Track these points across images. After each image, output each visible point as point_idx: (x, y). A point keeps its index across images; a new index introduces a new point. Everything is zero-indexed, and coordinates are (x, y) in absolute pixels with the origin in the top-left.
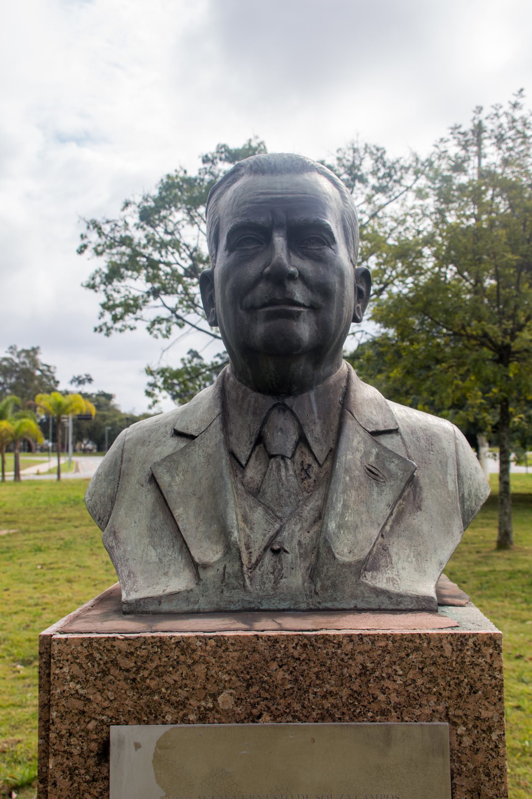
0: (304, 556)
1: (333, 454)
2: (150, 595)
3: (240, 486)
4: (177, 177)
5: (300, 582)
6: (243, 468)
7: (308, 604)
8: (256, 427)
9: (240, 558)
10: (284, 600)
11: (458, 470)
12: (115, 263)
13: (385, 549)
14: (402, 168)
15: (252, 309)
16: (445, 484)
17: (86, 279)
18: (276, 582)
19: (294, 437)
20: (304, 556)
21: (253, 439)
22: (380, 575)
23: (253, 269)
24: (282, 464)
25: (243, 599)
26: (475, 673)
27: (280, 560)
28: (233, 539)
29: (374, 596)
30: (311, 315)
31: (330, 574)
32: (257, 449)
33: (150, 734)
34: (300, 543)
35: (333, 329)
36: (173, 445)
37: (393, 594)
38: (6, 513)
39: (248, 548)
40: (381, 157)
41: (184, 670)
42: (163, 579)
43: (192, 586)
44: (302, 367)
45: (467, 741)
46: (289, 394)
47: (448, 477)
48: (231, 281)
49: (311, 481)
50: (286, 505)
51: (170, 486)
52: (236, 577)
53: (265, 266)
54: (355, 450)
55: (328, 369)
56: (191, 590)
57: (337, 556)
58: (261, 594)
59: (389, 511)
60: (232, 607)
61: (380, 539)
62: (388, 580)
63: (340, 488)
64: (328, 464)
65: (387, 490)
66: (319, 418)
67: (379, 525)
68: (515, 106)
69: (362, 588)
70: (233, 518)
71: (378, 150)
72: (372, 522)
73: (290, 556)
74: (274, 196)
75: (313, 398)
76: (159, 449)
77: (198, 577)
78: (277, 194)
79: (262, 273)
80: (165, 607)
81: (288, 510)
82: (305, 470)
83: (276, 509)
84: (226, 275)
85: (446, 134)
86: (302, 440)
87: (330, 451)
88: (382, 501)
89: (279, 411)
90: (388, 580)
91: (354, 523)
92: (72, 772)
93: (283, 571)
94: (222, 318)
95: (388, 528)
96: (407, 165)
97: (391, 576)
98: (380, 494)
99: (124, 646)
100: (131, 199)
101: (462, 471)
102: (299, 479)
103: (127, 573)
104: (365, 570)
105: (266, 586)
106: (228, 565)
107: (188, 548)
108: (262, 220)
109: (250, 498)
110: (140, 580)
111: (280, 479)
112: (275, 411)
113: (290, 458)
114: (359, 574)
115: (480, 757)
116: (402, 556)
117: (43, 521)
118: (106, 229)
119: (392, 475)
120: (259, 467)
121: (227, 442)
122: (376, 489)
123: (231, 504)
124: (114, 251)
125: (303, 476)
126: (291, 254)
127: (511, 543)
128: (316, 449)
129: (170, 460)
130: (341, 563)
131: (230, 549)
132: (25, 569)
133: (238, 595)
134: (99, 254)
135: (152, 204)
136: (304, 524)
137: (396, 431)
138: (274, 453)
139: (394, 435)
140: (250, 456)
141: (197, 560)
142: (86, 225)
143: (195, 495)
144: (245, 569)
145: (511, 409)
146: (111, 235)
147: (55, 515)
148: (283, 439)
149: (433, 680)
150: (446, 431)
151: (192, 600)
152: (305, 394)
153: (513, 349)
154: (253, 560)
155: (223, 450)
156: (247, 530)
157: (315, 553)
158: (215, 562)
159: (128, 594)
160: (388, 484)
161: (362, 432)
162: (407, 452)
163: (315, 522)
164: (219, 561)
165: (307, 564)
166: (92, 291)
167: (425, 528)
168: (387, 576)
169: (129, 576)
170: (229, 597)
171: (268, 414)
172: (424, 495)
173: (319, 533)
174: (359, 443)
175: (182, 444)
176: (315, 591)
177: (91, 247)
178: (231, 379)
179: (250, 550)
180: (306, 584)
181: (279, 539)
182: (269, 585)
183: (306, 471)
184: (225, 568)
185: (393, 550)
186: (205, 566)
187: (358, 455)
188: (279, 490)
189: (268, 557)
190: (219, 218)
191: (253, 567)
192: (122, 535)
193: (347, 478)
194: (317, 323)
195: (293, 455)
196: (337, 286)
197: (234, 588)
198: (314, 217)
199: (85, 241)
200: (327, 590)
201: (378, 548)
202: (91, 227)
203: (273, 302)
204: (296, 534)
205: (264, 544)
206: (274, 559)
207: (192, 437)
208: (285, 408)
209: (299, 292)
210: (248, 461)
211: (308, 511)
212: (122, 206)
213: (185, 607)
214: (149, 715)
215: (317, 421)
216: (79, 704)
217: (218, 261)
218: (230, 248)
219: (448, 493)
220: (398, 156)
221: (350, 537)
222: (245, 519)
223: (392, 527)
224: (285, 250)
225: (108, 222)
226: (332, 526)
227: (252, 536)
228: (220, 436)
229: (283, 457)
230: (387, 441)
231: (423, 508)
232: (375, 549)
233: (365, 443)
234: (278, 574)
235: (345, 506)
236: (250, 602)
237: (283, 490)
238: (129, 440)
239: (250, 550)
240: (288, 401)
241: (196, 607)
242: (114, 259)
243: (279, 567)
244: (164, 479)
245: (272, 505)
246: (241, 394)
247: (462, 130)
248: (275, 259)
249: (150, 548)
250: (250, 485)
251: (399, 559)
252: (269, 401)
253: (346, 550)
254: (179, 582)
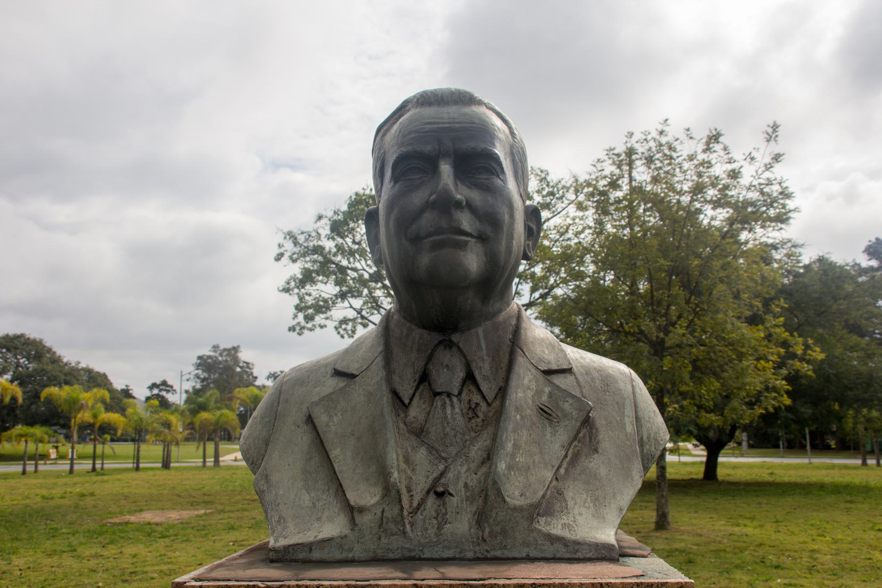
0: (470, 499)
1: (503, 392)
2: (300, 541)
3: (402, 425)
4: (364, 195)
5: (467, 528)
6: (406, 407)
7: (475, 552)
8: (421, 364)
9: (400, 501)
10: (449, 548)
11: (636, 412)
12: (309, 269)
13: (560, 493)
14: (563, 187)
15: (416, 240)
16: (623, 426)
17: (282, 283)
18: (440, 528)
19: (461, 374)
20: (470, 499)
21: (417, 377)
22: (554, 521)
23: (418, 198)
24: (448, 402)
25: (402, 547)
27: (444, 504)
28: (392, 479)
29: (548, 543)
30: (479, 245)
31: (499, 519)
32: (421, 387)
34: (466, 485)
35: (502, 263)
36: (332, 384)
37: (569, 541)
38: (205, 495)
39: (409, 490)
40: (545, 178)
42: (316, 525)
43: (346, 531)
44: (470, 300)
46: (456, 329)
47: (626, 418)
48: (396, 211)
49: (479, 420)
50: (452, 445)
51: (327, 425)
52: (396, 522)
53: (431, 195)
54: (525, 389)
55: (497, 305)
56: (346, 536)
57: (507, 499)
58: (422, 541)
59: (563, 453)
60: (391, 556)
61: (554, 482)
62: (564, 525)
63: (511, 427)
64: (497, 403)
65: (561, 431)
66: (488, 355)
67: (553, 467)
68: (661, 133)
69: (535, 534)
70: (393, 457)
71: (542, 171)
72: (546, 464)
73: (455, 500)
74: (441, 125)
75: (481, 334)
76: (318, 389)
77: (353, 522)
78: (443, 123)
79: (427, 202)
80: (316, 555)
81: (453, 450)
82: (473, 410)
83: (441, 449)
84: (390, 207)
85: (602, 155)
86: (470, 377)
87: (500, 389)
88: (556, 441)
89: (445, 348)
90: (564, 526)
91: (526, 462)
93: (448, 516)
94: (386, 252)
95: (562, 471)
96: (568, 185)
97: (567, 522)
98: (553, 434)
100: (324, 213)
101: (640, 414)
102: (466, 419)
103: (276, 518)
104: (538, 515)
105: (429, 532)
106: (386, 508)
107: (343, 491)
108: (428, 148)
109: (413, 438)
110: (291, 526)
111: (446, 417)
112: (441, 348)
113: (457, 396)
114: (531, 519)
116: (578, 501)
117: (237, 502)
118: (301, 239)
119: (566, 415)
120: (424, 406)
121: (389, 379)
122: (549, 429)
123: (392, 443)
124: (308, 259)
125: (471, 415)
126: (458, 183)
127: (668, 524)
128: (484, 387)
129: (329, 400)
130: (512, 507)
131: (389, 492)
132: (218, 545)
134: (294, 261)
135: (341, 217)
136: (471, 465)
137: (569, 371)
138: (439, 390)
139: (568, 375)
140: (414, 395)
141: (352, 503)
142: (283, 236)
143: (353, 435)
144: (405, 513)
145: (666, 400)
146: (306, 245)
147: (248, 497)
148: (448, 375)
150: (623, 374)
151: (346, 547)
152: (473, 331)
153: (667, 345)
154: (415, 504)
155: (384, 388)
156: (409, 472)
157: (483, 496)
158: (373, 505)
159: (276, 540)
160: (562, 424)
161: (533, 370)
162: (582, 392)
163: (483, 463)
164: (377, 504)
165: (474, 509)
166: (287, 294)
167: (603, 471)
168: (563, 521)
169: (279, 521)
170: (388, 544)
171: (434, 351)
172: (601, 437)
173: (487, 475)
174: (530, 381)
175: (341, 383)
176: (483, 538)
177: (287, 255)
178: (395, 316)
179: (412, 493)
180: (472, 530)
181: (443, 480)
182: (432, 531)
183: (473, 410)
184: (383, 512)
185: (569, 494)
186: (362, 510)
187: (530, 394)
188: (444, 428)
189: (431, 500)
190: (385, 152)
191: (415, 511)
192: (275, 478)
193: (518, 417)
194: (486, 254)
195: (460, 393)
196: (507, 217)
197: (393, 535)
198: (482, 146)
199: (282, 250)
200: (496, 537)
201: (552, 492)
202: (288, 237)
204: (462, 477)
205: (427, 487)
206: (438, 503)
207: (353, 376)
208: (450, 345)
209: (466, 221)
210: (411, 400)
211: (476, 451)
212: (314, 219)
213: (338, 556)
215: (486, 358)
217: (383, 194)
218: (395, 179)
219: (626, 435)
220: (560, 177)
221: (521, 479)
222: (407, 460)
223: (567, 470)
224: (452, 177)
225: (302, 233)
226: (502, 466)
227: (414, 478)
228: (382, 374)
229: (449, 395)
230: (559, 380)
231: (600, 451)
232: (549, 492)
233: (537, 381)
234: (442, 519)
235: (516, 446)
236: (410, 550)
237: (448, 429)
238: (287, 381)
239: (412, 493)
240: (455, 338)
241: (350, 555)
242: (307, 266)
243: (443, 511)
244: (322, 419)
245: (436, 445)
246: (405, 331)
247: (616, 152)
248: (441, 186)
249: (304, 491)
250: (414, 425)
251: (575, 504)
253: (517, 493)
254: (332, 527)
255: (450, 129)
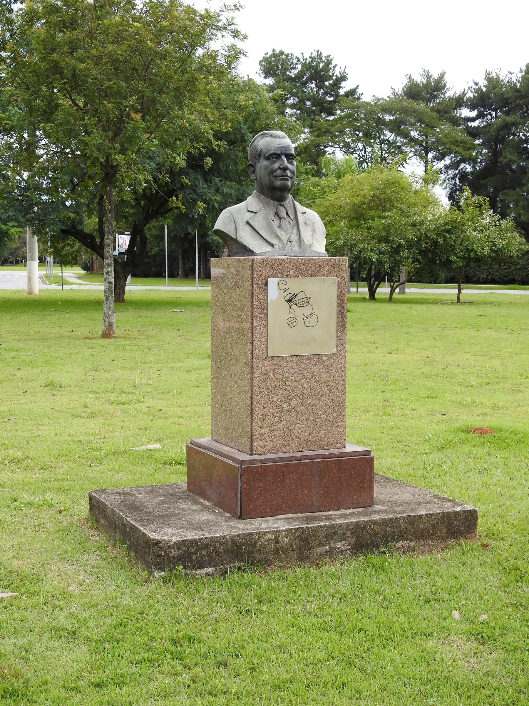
15: (275, 177)
20: (297, 243)
23: (276, 165)
26: (342, 266)
33: (276, 280)
41: (283, 265)
45: (340, 281)
92: (259, 288)
99: (270, 260)
108: (279, 152)
115: (342, 285)
133: (284, 252)
148: (283, 214)
149: (334, 268)
175: (252, 214)
182: (290, 249)
203: (283, 176)
207: (256, 213)
208: (281, 205)
214: (276, 276)
216: (261, 273)
240: (282, 203)
252: (277, 203)
255: (286, 147)
